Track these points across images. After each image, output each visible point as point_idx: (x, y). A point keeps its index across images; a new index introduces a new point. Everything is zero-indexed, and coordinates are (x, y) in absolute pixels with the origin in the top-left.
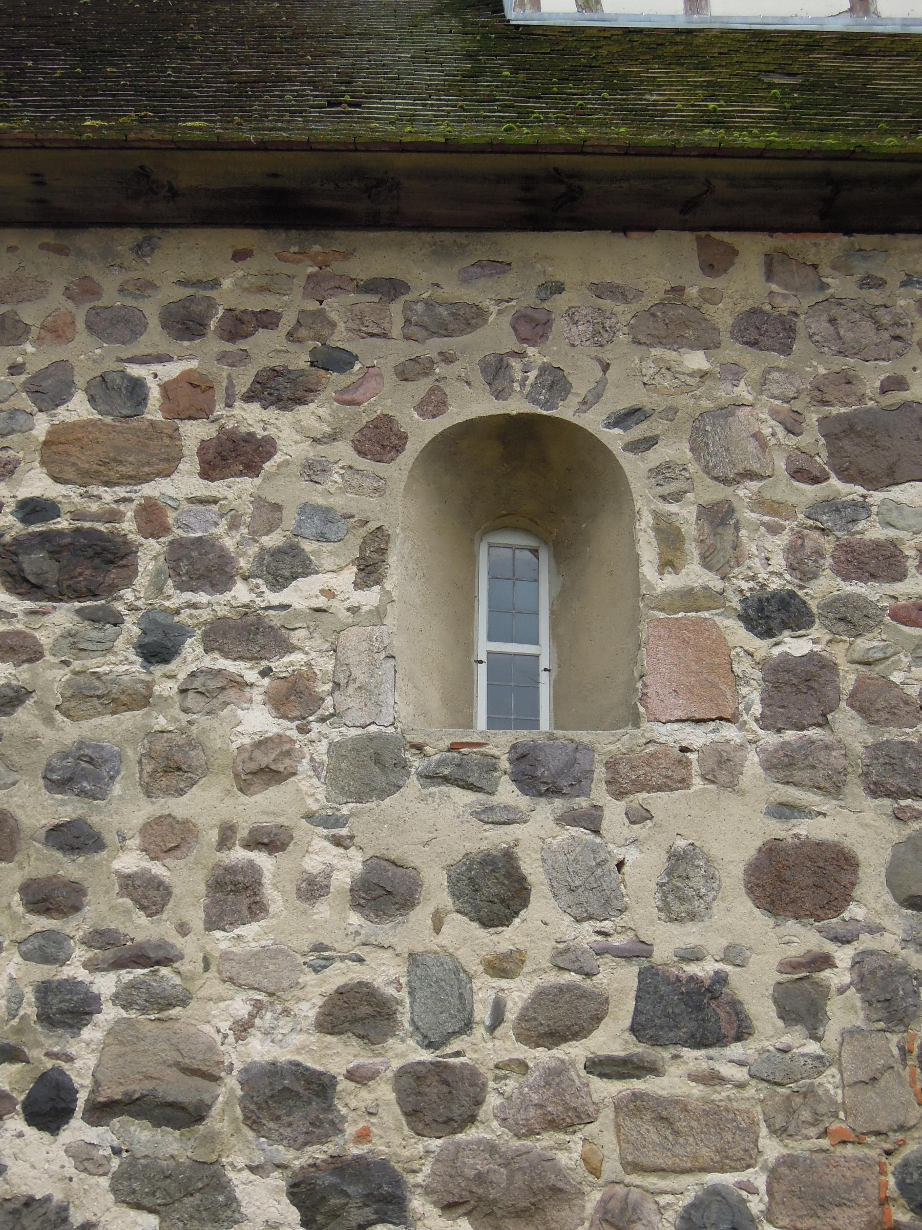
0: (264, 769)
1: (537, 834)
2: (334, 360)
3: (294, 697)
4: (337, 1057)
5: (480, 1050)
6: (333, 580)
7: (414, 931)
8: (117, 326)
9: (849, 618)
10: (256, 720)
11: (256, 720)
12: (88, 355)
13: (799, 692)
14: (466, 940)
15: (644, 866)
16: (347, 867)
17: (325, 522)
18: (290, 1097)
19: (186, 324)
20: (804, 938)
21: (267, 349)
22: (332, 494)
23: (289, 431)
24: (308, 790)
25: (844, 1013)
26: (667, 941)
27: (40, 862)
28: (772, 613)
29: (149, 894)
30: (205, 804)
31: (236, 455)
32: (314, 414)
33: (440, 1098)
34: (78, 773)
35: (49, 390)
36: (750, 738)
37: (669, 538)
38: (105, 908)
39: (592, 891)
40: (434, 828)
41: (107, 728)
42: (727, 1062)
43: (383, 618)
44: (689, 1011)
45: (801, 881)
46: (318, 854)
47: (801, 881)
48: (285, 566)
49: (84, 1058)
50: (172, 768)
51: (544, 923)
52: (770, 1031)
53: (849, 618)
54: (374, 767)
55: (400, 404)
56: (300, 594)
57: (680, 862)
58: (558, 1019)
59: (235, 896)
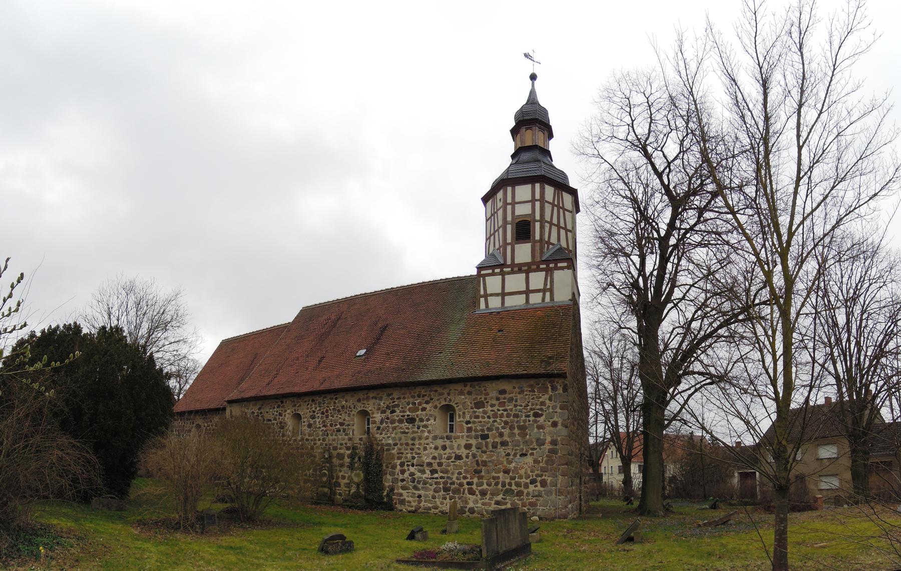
0: (427, 438)
1: (448, 443)
2: (432, 399)
3: (429, 432)
4: (433, 461)
5: (443, 461)
6: (432, 421)
7: (438, 451)
8: (413, 397)
9: (474, 422)
10: (426, 434)
11: (426, 434)
12: (411, 400)
13: (469, 430)
14: (442, 452)
15: (456, 445)
16: (433, 446)
17: (431, 415)
18: (429, 464)
19: (419, 396)
20: (468, 451)
21: (426, 398)
22: (432, 413)
23: (428, 406)
24: (430, 440)
25: (470, 457)
26: (457, 452)
27: (411, 447)
28: (468, 422)
29: (419, 449)
30: (423, 441)
31: (424, 409)
32: (430, 405)
33: (440, 464)
34: (413, 439)
35: (408, 404)
36: (465, 434)
37: (459, 415)
38: (416, 450)
39: (452, 448)
40: (440, 443)
41: (415, 435)
42: (461, 461)
43: (436, 424)
44: (458, 457)
45: (468, 447)
46: (431, 445)
47: (468, 447)
48: (428, 420)
49: (415, 462)
50: (420, 438)
51: (448, 450)
52: (465, 459)
53: (474, 422)
54: (435, 438)
55: (437, 403)
56: (429, 423)
57: (459, 445)
58: (449, 458)
59: (425, 449)
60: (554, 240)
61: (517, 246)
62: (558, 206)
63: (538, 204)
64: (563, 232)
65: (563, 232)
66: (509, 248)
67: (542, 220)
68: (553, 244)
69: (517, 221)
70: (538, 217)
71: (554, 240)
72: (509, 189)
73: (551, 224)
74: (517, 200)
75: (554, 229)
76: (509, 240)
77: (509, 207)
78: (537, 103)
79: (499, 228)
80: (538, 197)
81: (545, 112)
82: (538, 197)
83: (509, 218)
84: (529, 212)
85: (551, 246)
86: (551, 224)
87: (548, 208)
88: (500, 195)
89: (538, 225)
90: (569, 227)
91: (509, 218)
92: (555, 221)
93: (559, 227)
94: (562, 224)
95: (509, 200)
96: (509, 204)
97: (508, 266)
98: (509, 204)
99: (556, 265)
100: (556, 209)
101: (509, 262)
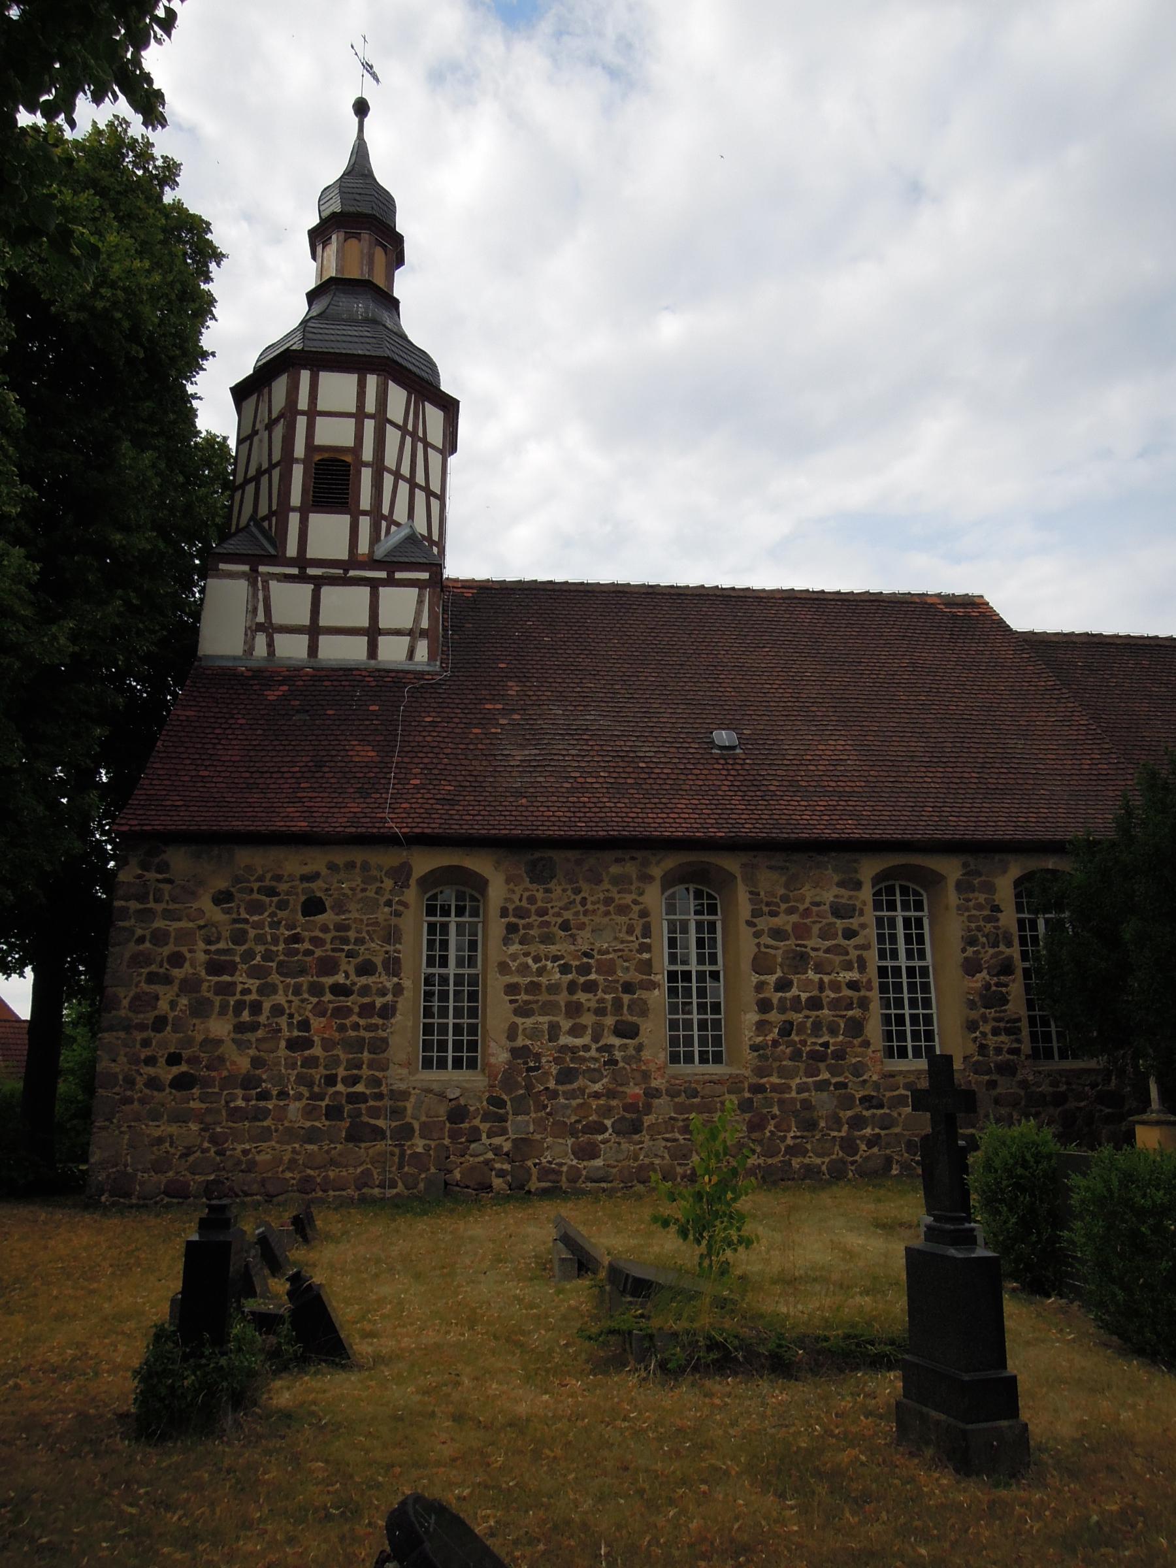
60: (401, 515)
61: (315, 519)
62: (414, 434)
63: (369, 425)
64: (420, 496)
65: (420, 496)
66: (294, 519)
67: (379, 468)
68: (398, 525)
69: (317, 458)
70: (368, 454)
71: (401, 515)
72: (305, 375)
73: (397, 475)
74: (321, 406)
75: (404, 487)
76: (296, 499)
77: (301, 422)
78: (370, 175)
79: (272, 466)
80: (370, 407)
81: (386, 202)
82: (370, 407)
83: (299, 451)
84: (350, 443)
85: (393, 528)
86: (397, 475)
87: (393, 436)
88: (280, 386)
89: (366, 474)
90: (435, 487)
91: (299, 451)
92: (405, 470)
93: (413, 485)
94: (420, 479)
95: (303, 404)
96: (303, 413)
97: (290, 562)
98: (303, 413)
99: (391, 574)
100: (408, 439)
101: (292, 551)
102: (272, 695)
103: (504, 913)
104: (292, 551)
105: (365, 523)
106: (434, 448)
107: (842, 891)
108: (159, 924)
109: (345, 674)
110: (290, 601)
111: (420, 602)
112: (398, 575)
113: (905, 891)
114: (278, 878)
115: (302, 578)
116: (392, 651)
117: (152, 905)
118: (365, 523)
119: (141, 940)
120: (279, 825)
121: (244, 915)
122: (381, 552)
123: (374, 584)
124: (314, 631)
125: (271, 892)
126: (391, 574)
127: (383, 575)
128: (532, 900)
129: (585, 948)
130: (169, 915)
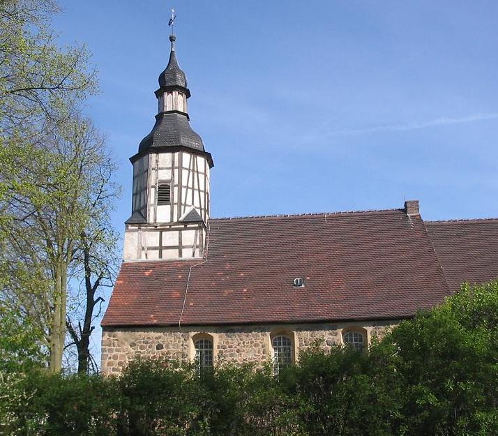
60: (189, 202)
63: (176, 171)
65: (196, 193)
66: (152, 209)
67: (180, 186)
70: (176, 182)
71: (189, 202)
73: (187, 187)
75: (190, 191)
80: (176, 164)
82: (176, 164)
87: (185, 173)
89: (176, 189)
92: (190, 185)
93: (193, 189)
102: (147, 273)
103: (218, 347)
104: (151, 220)
105: (176, 207)
106: (201, 173)
107: (331, 336)
108: (115, 353)
109: (171, 263)
110: (152, 239)
111: (196, 235)
112: (188, 226)
113: (356, 335)
114: (149, 338)
115: (156, 230)
116: (187, 254)
117: (112, 347)
118: (176, 207)
119: (110, 358)
120: (149, 322)
121: (139, 350)
122: (180, 219)
123: (180, 230)
124: (161, 248)
125: (147, 343)
126: (185, 226)
127: (183, 226)
128: (227, 343)
129: (245, 358)
130: (118, 350)
